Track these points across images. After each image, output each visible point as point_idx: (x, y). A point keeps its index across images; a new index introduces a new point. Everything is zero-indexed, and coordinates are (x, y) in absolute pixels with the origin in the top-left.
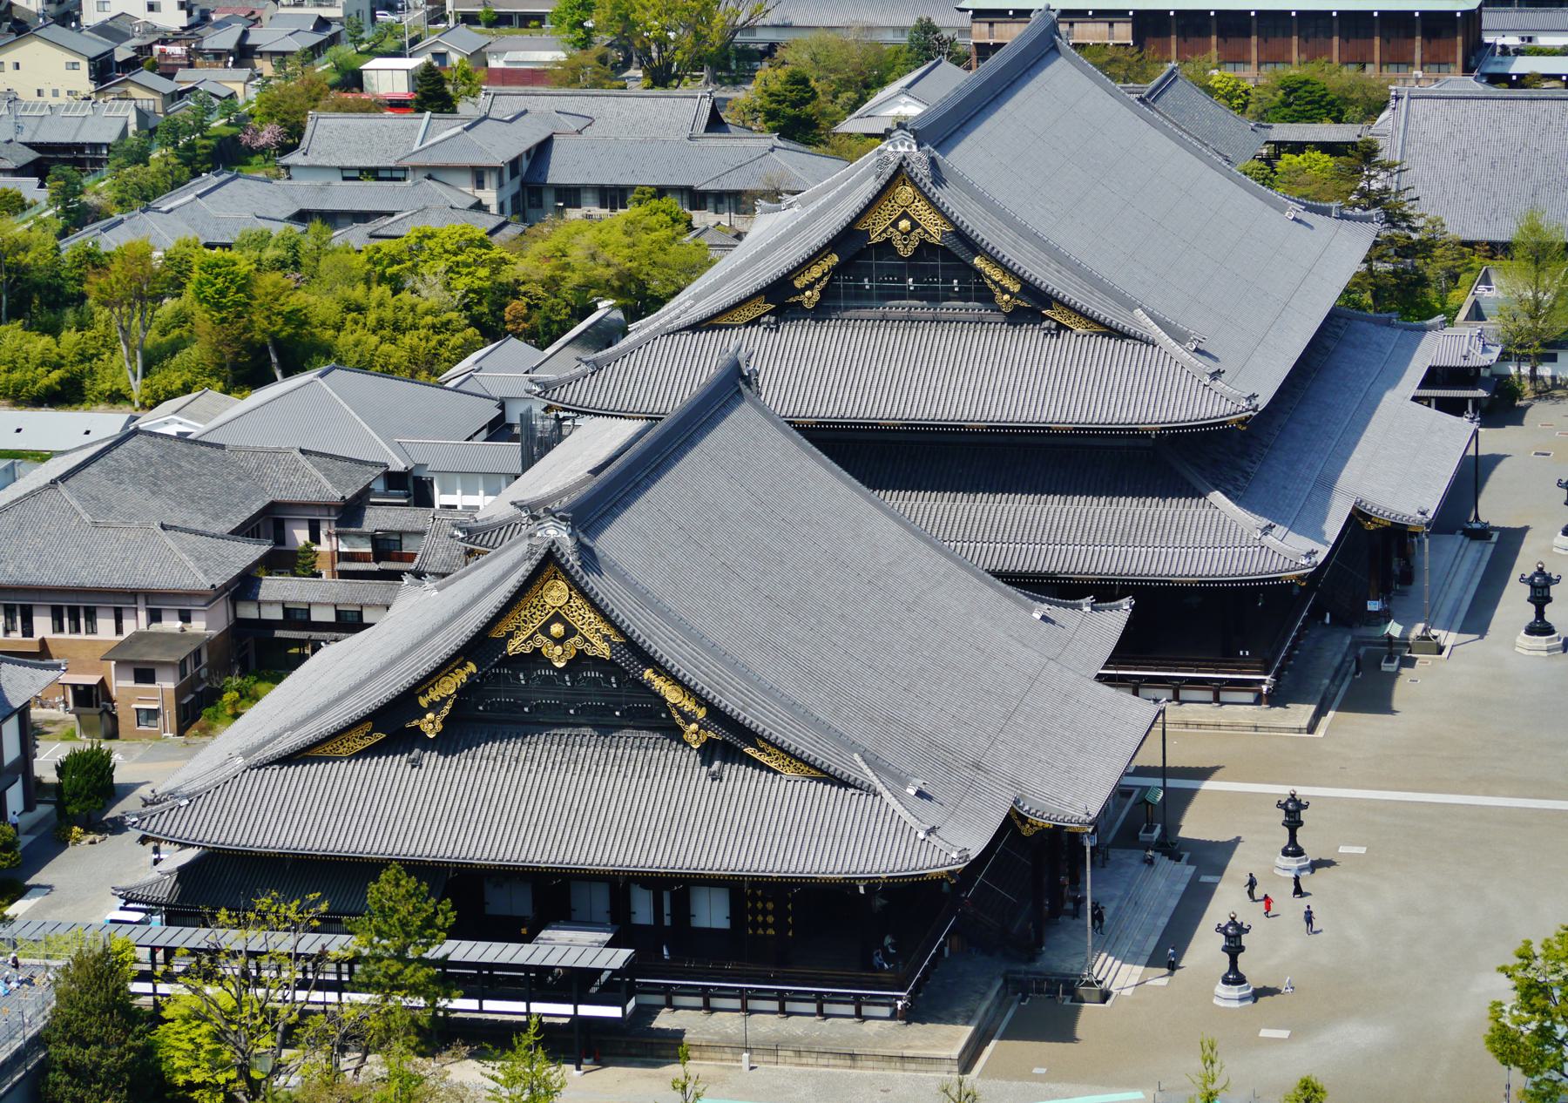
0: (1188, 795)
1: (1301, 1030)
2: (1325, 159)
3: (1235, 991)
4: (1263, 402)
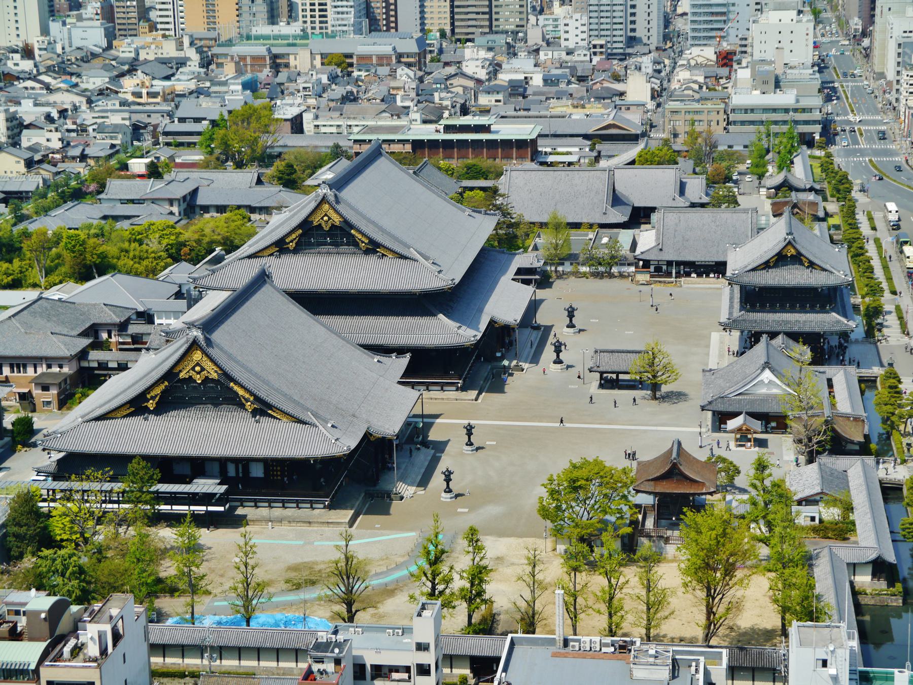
0: (432, 424)
1: (472, 509)
3: (449, 495)
4: (457, 281)
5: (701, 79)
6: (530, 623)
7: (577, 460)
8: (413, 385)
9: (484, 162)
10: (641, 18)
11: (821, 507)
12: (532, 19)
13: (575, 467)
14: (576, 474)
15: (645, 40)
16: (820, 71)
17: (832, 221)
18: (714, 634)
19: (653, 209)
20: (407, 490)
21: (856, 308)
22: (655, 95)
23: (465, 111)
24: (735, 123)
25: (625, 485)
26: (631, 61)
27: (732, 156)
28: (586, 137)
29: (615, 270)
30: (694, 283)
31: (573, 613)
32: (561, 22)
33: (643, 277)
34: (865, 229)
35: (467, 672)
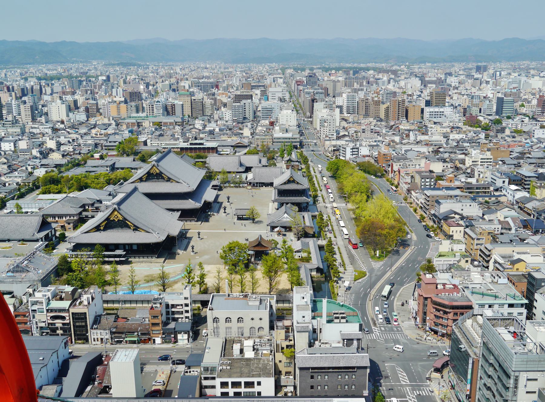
1: (200, 257)
2: (201, 163)
3: (193, 253)
4: (194, 189)
5: (265, 130)
6: (218, 290)
7: (231, 242)
8: (182, 220)
9: (202, 154)
10: (247, 112)
11: (302, 253)
12: (215, 112)
13: (230, 243)
14: (231, 246)
15: (248, 118)
16: (299, 127)
17: (303, 170)
18: (272, 291)
19: (252, 167)
20: (180, 252)
21: (310, 195)
22: (252, 134)
23: (196, 139)
24: (275, 142)
25: (245, 248)
26: (245, 124)
27: (274, 152)
28: (232, 146)
29: (241, 185)
30: (264, 189)
31: (231, 286)
32: (224, 113)
33: (249, 187)
34: (312, 173)
35: (200, 305)
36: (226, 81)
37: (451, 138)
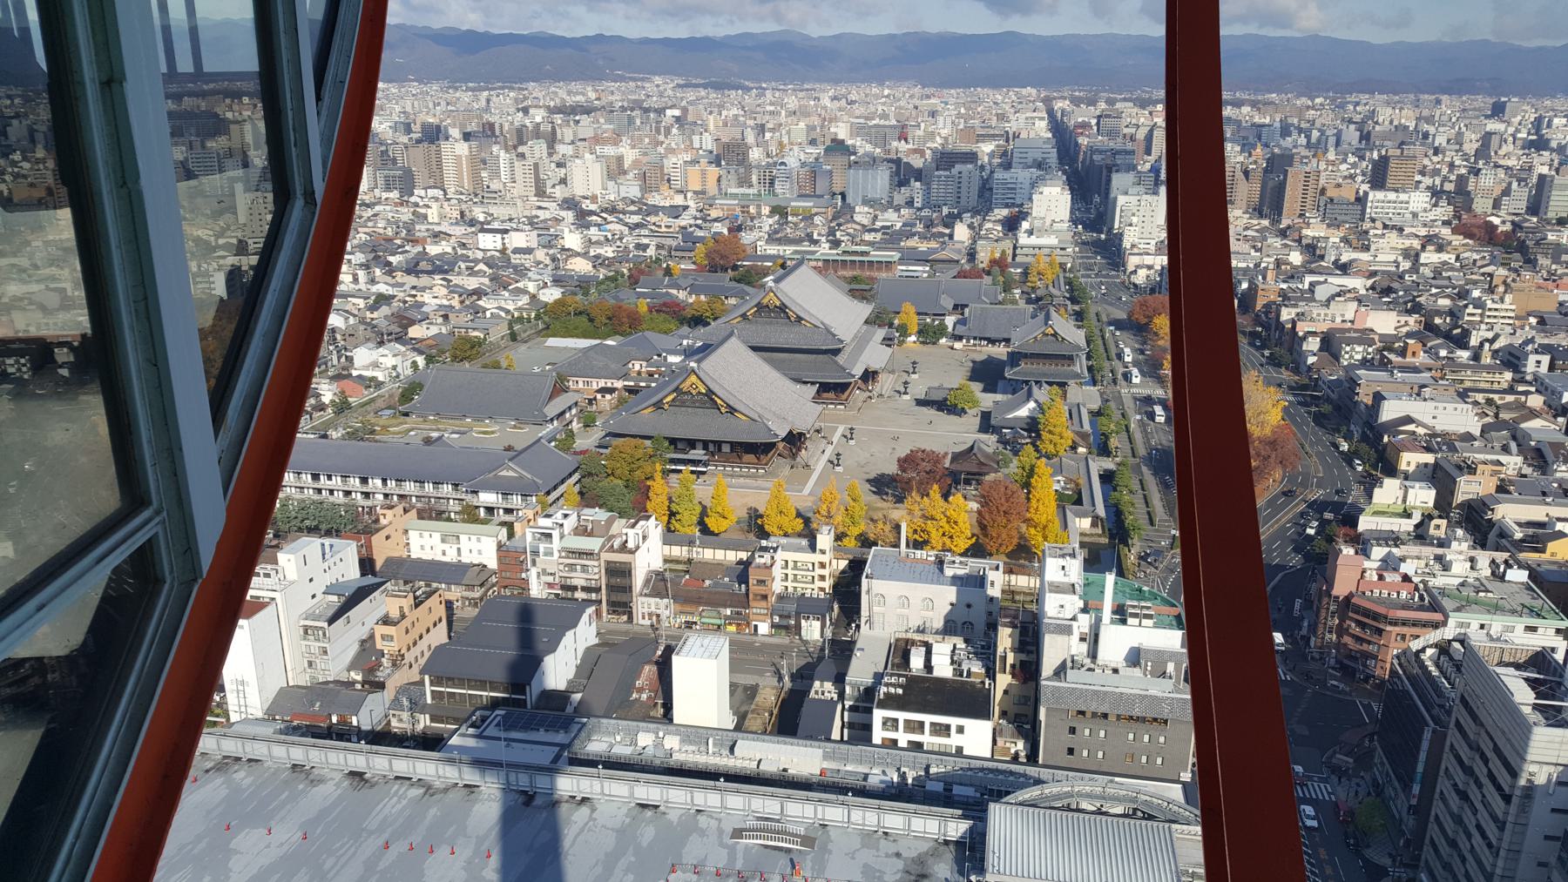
36: (923, 125)
37: (1422, 260)
